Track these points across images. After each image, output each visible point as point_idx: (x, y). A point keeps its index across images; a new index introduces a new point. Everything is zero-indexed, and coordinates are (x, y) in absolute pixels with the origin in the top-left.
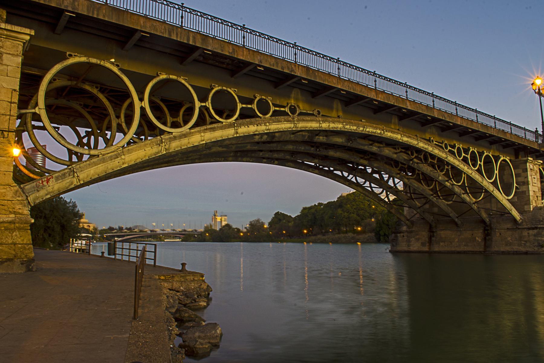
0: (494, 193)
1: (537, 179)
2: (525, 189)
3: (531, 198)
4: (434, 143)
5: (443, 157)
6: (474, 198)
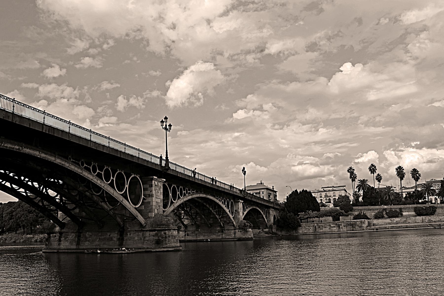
0: (123, 203)
1: (161, 193)
2: (150, 201)
3: (154, 207)
4: (72, 160)
5: (79, 172)
6: (111, 206)
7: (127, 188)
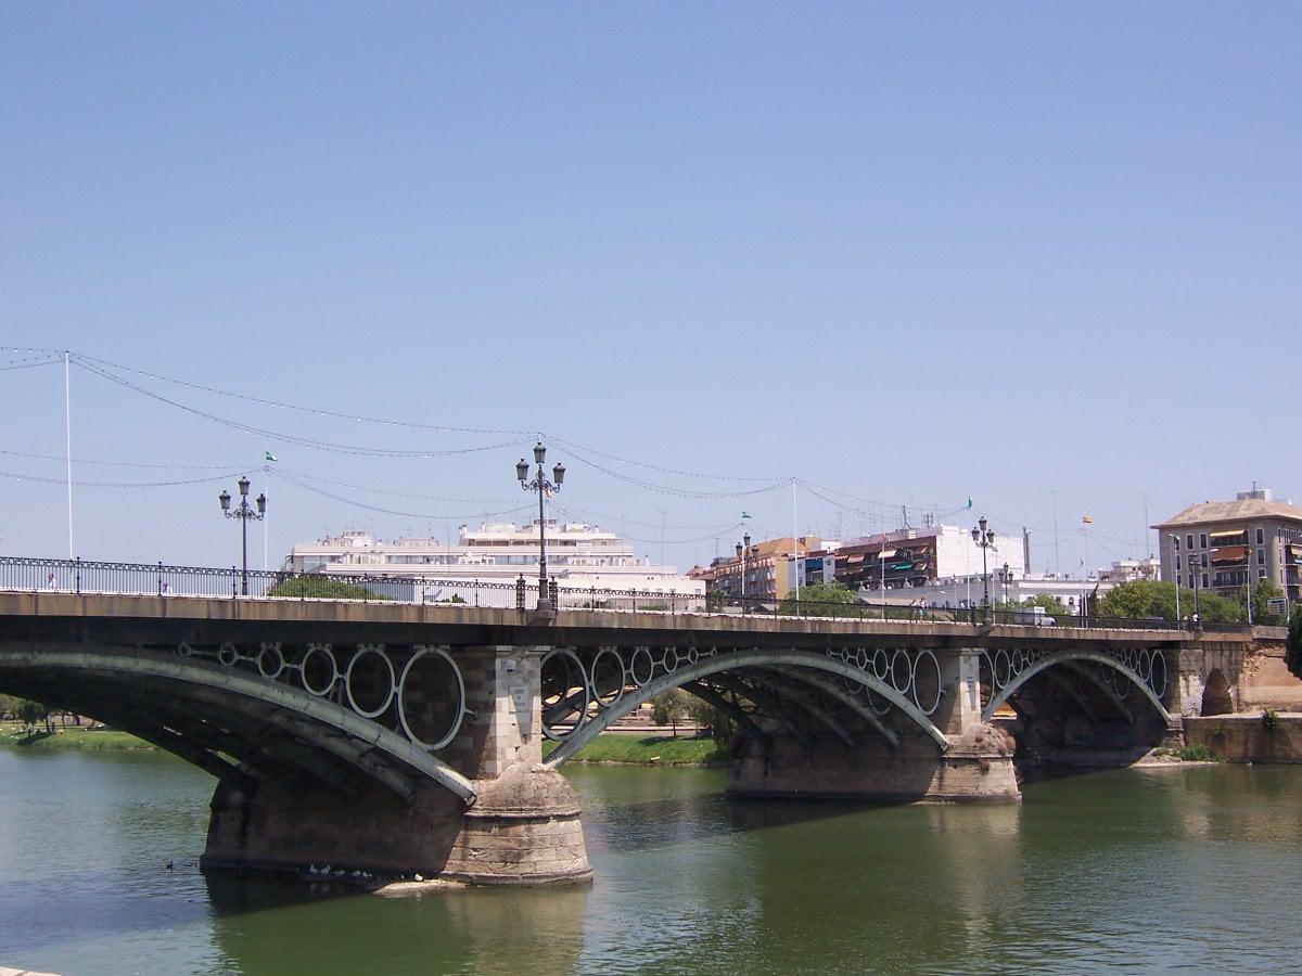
7: (396, 695)
